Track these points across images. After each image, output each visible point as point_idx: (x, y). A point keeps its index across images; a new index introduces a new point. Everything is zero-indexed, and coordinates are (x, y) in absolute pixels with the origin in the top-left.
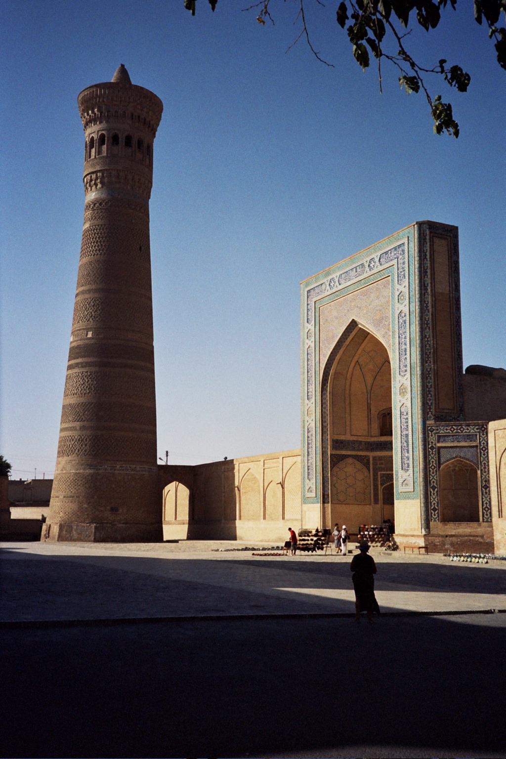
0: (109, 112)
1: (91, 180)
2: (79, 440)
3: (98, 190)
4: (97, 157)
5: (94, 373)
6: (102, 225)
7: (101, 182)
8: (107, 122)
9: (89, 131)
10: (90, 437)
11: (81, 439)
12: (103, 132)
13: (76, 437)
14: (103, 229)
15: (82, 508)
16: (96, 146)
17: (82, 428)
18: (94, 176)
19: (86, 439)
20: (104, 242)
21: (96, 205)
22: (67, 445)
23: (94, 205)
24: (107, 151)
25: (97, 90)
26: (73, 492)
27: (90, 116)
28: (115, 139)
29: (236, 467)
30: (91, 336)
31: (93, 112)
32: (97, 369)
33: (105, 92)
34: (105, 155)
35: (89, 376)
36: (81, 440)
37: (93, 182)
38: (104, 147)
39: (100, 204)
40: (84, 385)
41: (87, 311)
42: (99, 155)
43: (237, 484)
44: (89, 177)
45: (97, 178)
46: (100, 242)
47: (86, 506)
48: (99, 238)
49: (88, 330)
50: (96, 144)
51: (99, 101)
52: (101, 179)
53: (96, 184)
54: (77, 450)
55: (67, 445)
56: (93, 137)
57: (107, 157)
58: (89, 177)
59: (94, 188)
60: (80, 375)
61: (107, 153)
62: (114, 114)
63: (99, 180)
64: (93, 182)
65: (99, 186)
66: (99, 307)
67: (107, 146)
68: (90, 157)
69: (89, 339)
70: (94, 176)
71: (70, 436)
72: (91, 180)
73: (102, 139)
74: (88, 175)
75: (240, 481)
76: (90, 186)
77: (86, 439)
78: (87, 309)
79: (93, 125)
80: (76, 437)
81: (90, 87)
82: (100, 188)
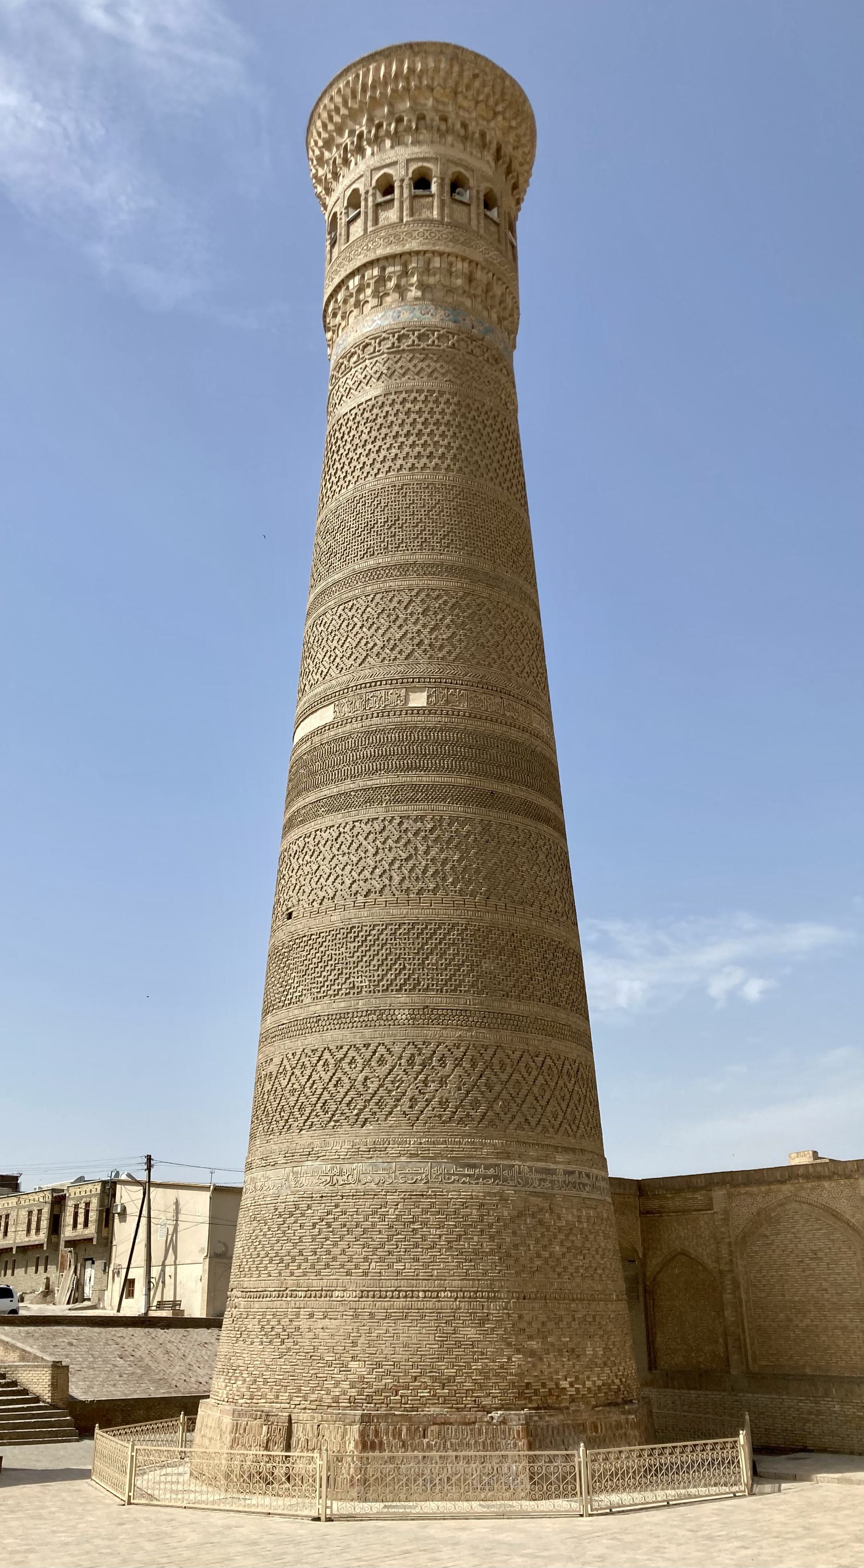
2: (411, 1061)
5: (450, 825)
10: (458, 1053)
11: (418, 1060)
13: (397, 1049)
15: (458, 1344)
17: (424, 1015)
19: (442, 1059)
30: (425, 705)
35: (432, 831)
36: (420, 1060)
41: (400, 627)
47: (470, 1333)
49: (411, 684)
50: (402, 192)
54: (405, 1100)
64: (391, 284)
65: (414, 293)
69: (418, 711)
71: (367, 1046)
74: (370, 264)
77: (442, 1059)
80: (397, 1049)
82: (416, 299)
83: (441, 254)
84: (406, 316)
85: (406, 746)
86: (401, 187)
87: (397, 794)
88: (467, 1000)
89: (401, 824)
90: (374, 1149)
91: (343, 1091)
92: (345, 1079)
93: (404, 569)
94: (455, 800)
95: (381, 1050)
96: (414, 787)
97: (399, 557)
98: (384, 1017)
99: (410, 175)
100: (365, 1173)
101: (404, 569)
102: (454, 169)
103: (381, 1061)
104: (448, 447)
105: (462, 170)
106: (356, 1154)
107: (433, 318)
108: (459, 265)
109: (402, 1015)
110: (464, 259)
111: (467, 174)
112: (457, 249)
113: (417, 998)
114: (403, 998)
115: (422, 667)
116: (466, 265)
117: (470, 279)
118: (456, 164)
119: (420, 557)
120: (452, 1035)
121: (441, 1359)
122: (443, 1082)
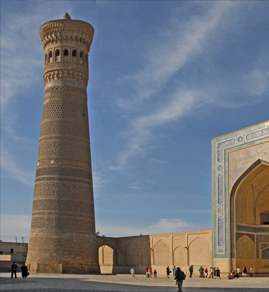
0: (61, 36)
1: (50, 75)
2: (48, 220)
3: (55, 81)
4: (54, 62)
5: (56, 184)
6: (58, 101)
7: (57, 77)
8: (61, 42)
9: (48, 47)
10: (55, 219)
11: (49, 219)
12: (58, 48)
14: (59, 103)
16: (53, 56)
18: (52, 73)
20: (60, 110)
21: (54, 90)
22: (39, 222)
23: (53, 89)
24: (61, 59)
25: (54, 24)
26: (46, 247)
27: (49, 39)
28: (66, 53)
29: (151, 239)
30: (53, 163)
31: (51, 36)
32: (58, 181)
33: (59, 25)
34: (60, 61)
35: (53, 185)
37: (52, 77)
38: (59, 57)
39: (57, 89)
40: (49, 190)
41: (49, 149)
42: (55, 61)
43: (151, 247)
44: (48, 74)
45: (54, 75)
46: (57, 110)
48: (56, 108)
50: (54, 55)
51: (55, 30)
52: (57, 75)
53: (53, 78)
54: (46, 225)
55: (39, 222)
56: (51, 51)
57: (61, 62)
58: (48, 74)
59: (52, 80)
60: (46, 184)
61: (61, 60)
62: (65, 38)
63: (56, 76)
64: (52, 77)
65: (56, 79)
66: (58, 147)
67: (61, 57)
68: (49, 62)
69: (52, 164)
70: (52, 73)
71: (41, 217)
72: (50, 75)
73: (57, 53)
74: (48, 72)
75: (153, 247)
76: (49, 78)
77: (53, 219)
78: (49, 148)
79: (51, 44)
80: (46, 218)
81: (49, 22)
82: (56, 80)
83: (61, 70)
84: (54, 85)
85: (50, 171)
86: (53, 54)
87: (47, 179)
88: (57, 211)
89: (48, 184)
90: (42, 231)
91: (38, 223)
92: (38, 222)
93: (51, 138)
94: (57, 180)
95: (43, 218)
96: (50, 178)
97: (50, 135)
98: (44, 213)
99: (55, 51)
100: (41, 234)
101: (51, 138)
102: (64, 48)
103: (43, 220)
104: (61, 113)
105: (66, 48)
106: (39, 232)
107: (59, 84)
108: (65, 71)
109: (46, 213)
110: (66, 70)
111: (68, 48)
112: (65, 68)
113: (49, 211)
114: (47, 210)
115: (53, 156)
116: (67, 71)
117: (68, 73)
118: (64, 47)
119: (54, 136)
120: (54, 216)
121: (50, 258)
122: (53, 223)
